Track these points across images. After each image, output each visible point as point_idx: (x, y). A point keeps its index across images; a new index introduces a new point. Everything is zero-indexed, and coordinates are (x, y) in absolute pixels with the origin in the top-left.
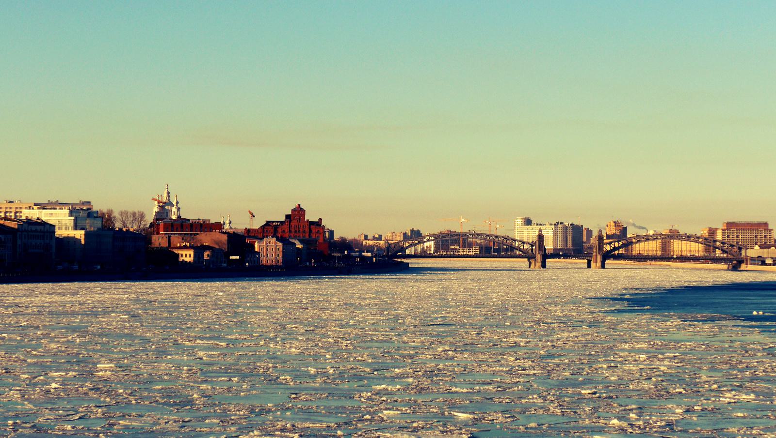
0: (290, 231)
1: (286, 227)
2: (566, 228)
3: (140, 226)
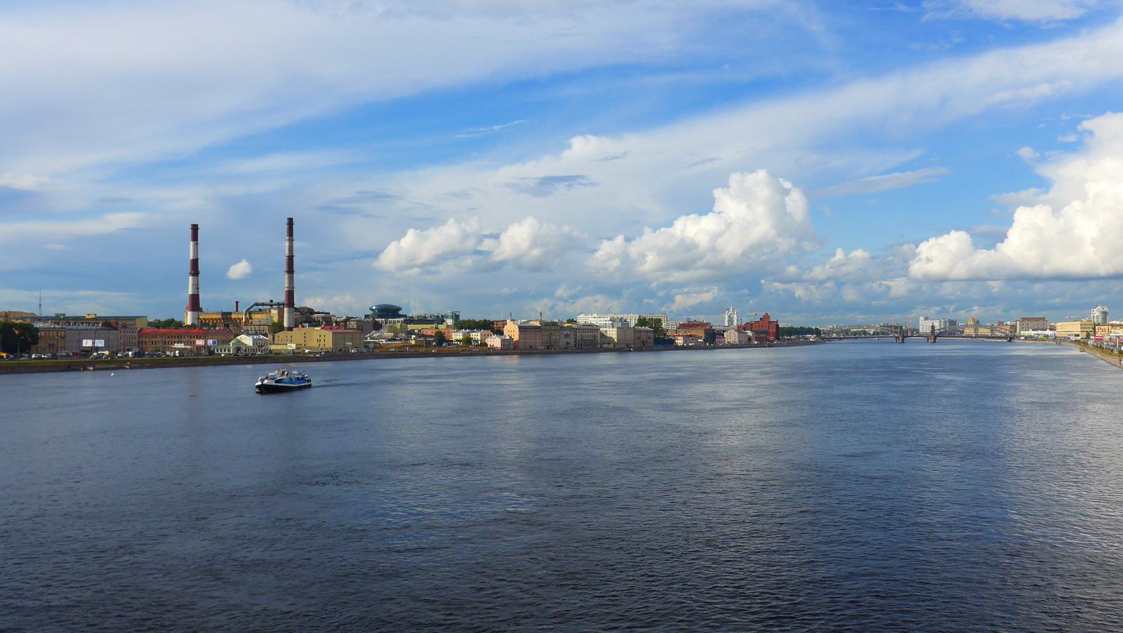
2: (945, 322)
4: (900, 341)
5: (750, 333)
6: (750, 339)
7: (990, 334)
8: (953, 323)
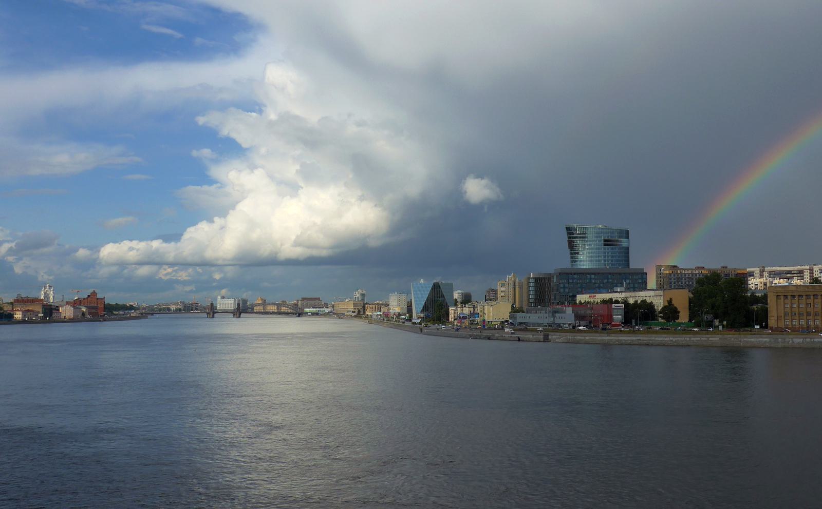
0: (87, 303)
1: (86, 300)
2: (239, 300)
4: (211, 316)
5: (84, 309)
6: (83, 314)
7: (276, 311)
8: (245, 301)
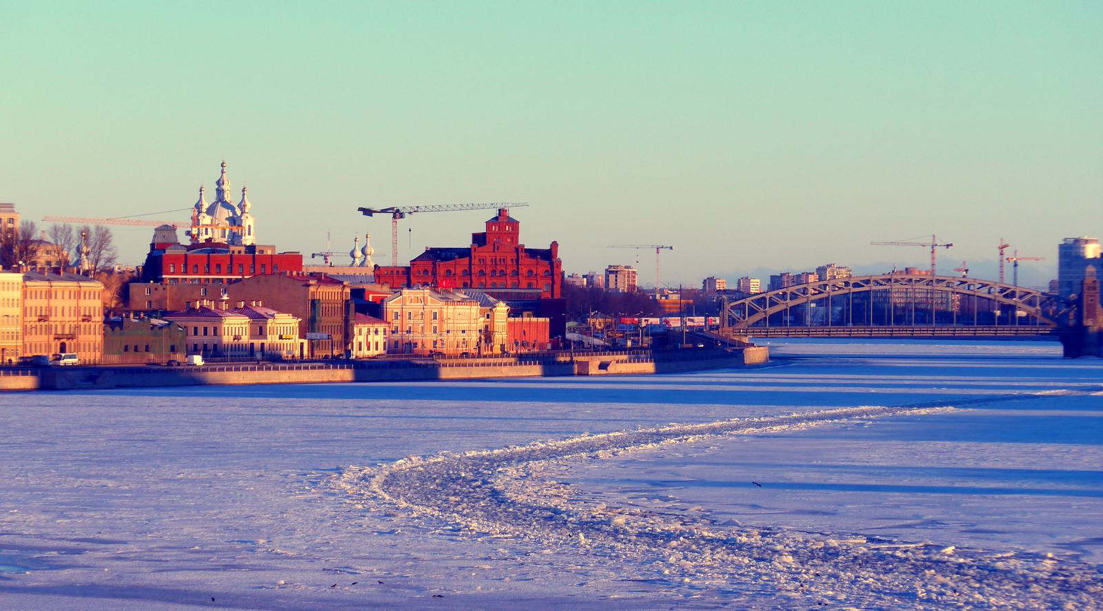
3: (97, 261)
